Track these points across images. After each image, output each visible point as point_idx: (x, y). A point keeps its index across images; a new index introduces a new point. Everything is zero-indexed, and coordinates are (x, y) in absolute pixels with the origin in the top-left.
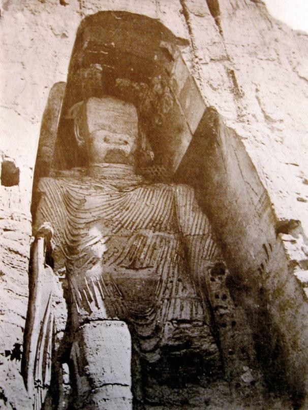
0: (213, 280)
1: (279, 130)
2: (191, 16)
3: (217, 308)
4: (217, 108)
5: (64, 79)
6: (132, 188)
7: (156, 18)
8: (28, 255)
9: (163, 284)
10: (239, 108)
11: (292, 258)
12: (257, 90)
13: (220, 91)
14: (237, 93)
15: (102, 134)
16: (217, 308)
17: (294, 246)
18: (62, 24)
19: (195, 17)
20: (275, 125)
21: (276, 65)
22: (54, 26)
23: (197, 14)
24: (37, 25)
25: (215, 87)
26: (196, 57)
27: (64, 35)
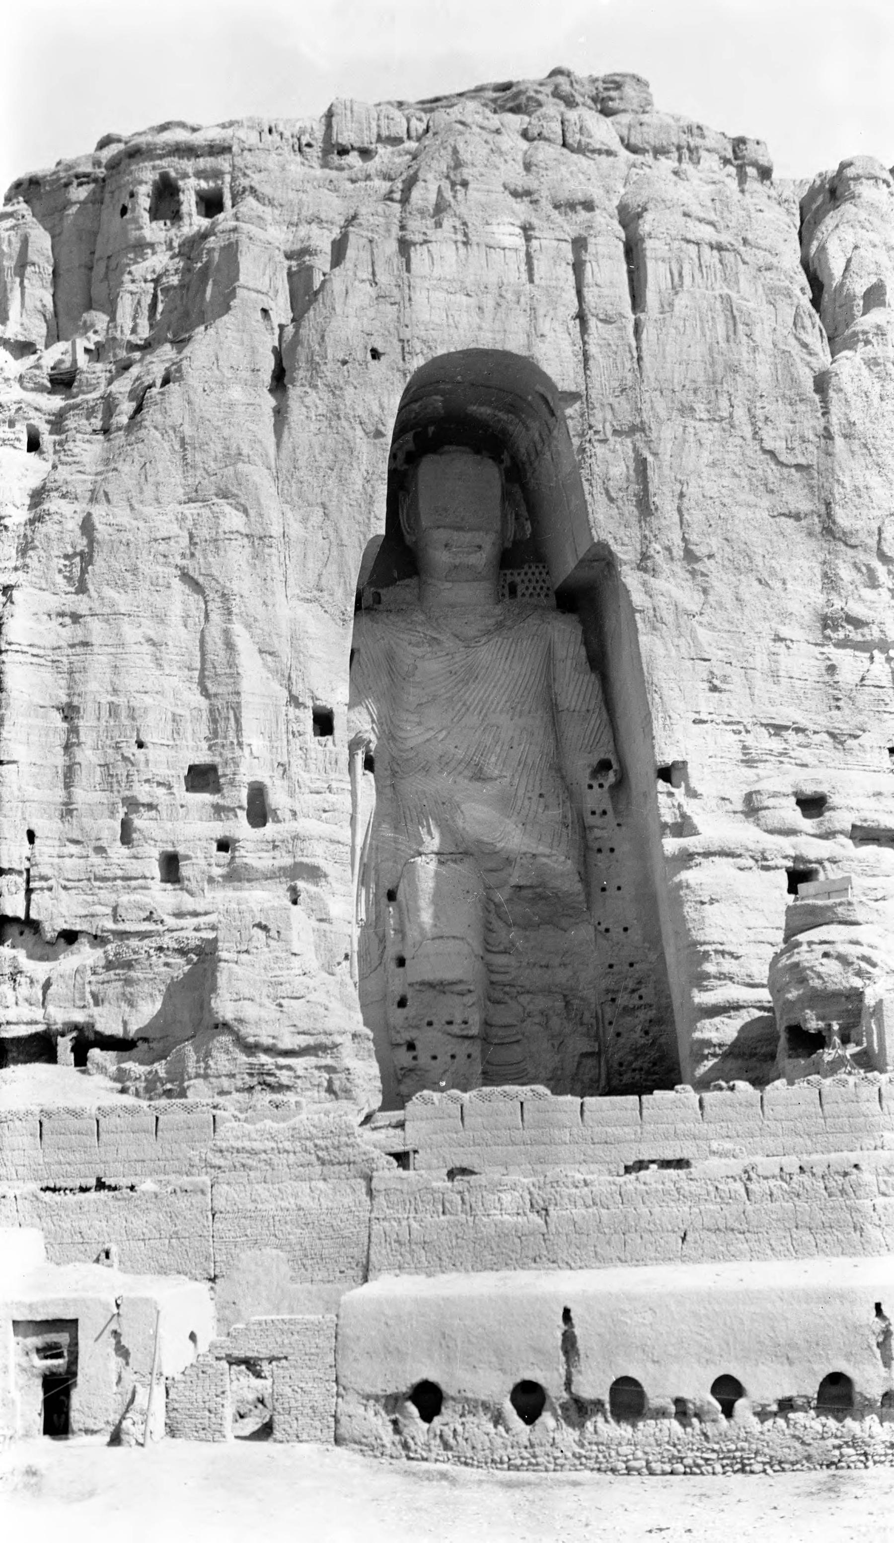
0: (590, 787)
1: (703, 574)
2: (593, 323)
3: (591, 828)
4: (611, 542)
5: (382, 532)
6: (484, 640)
7: (524, 353)
8: (349, 842)
9: (519, 803)
10: (645, 537)
11: (663, 819)
12: (682, 495)
13: (620, 503)
14: (645, 506)
15: (441, 535)
16: (591, 828)
17: (669, 801)
18: (376, 410)
19: (600, 324)
20: (698, 566)
21: (724, 430)
22: (365, 418)
23: (602, 316)
24: (339, 418)
25: (613, 495)
26: (591, 427)
27: (379, 434)
